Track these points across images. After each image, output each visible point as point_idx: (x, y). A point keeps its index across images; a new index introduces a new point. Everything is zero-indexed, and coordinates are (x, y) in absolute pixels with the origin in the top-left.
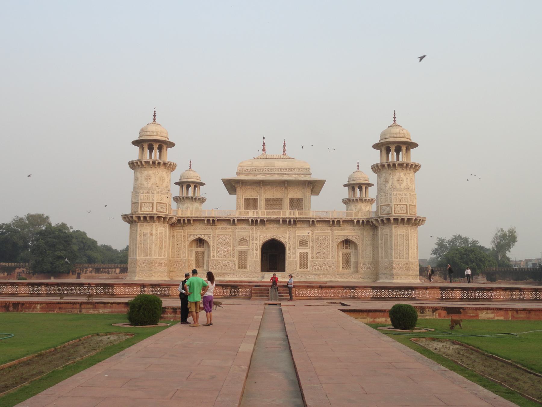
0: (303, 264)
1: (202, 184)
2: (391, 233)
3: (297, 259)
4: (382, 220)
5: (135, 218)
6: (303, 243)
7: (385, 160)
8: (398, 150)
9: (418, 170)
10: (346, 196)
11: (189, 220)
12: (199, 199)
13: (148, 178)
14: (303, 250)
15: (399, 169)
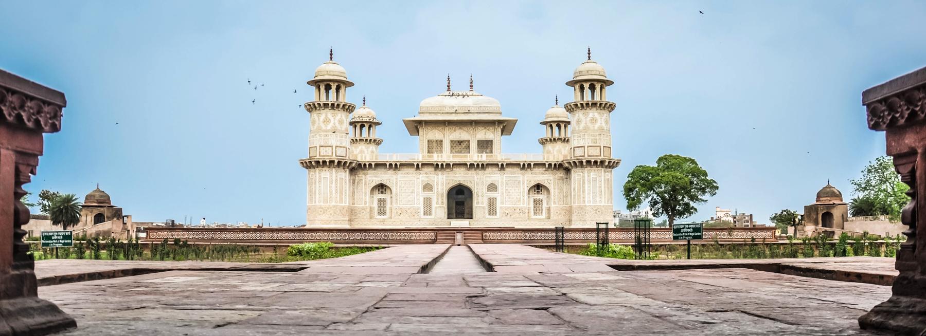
0: (492, 210)
1: (378, 124)
2: (583, 176)
3: (486, 205)
4: (575, 163)
5: (314, 164)
6: (492, 187)
7: (579, 99)
8: (592, 88)
9: (613, 109)
10: (545, 136)
11: (370, 165)
12: (375, 141)
13: (326, 121)
14: (492, 195)
15: (594, 109)
